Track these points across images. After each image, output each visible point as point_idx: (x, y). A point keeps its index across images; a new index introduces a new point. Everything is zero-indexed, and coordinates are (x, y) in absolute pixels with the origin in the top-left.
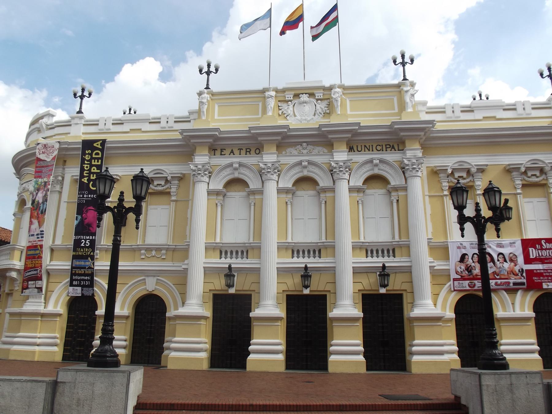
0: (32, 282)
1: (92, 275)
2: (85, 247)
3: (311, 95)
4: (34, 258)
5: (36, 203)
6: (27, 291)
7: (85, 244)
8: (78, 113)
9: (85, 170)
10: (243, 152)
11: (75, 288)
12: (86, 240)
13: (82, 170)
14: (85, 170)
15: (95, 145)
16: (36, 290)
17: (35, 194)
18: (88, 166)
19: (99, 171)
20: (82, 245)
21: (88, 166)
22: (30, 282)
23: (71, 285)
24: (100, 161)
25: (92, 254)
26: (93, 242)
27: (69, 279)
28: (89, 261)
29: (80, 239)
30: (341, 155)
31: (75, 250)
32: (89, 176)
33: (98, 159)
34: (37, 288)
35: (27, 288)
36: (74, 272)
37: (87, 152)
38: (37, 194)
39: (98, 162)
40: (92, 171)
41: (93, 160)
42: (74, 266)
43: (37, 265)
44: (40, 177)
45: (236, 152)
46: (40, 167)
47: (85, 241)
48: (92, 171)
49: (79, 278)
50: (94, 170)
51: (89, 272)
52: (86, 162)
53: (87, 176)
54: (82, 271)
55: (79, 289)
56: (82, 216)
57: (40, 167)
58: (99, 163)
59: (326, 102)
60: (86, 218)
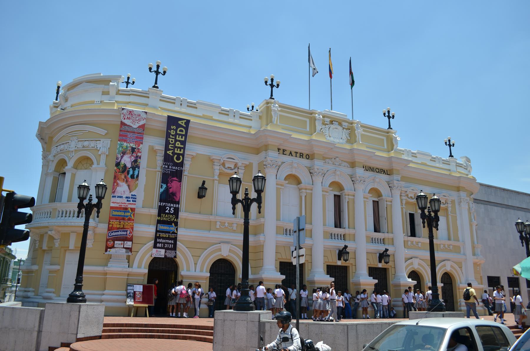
0: (120, 242)
1: (175, 239)
2: (169, 213)
3: (340, 124)
4: (124, 219)
5: (122, 166)
7: (169, 211)
8: (154, 87)
9: (170, 144)
10: (298, 155)
11: (159, 250)
12: (170, 208)
13: (167, 143)
14: (170, 144)
15: (180, 122)
16: (124, 250)
17: (119, 156)
18: (173, 140)
19: (182, 146)
20: (167, 211)
21: (173, 140)
22: (116, 242)
23: (155, 247)
24: (184, 137)
25: (175, 220)
26: (177, 211)
27: (153, 241)
28: (173, 227)
29: (165, 206)
30: (360, 172)
31: (159, 215)
32: (174, 150)
33: (182, 135)
34: (126, 248)
35: (113, 247)
36: (158, 235)
37: (172, 127)
38: (122, 157)
39: (182, 138)
40: (177, 145)
41: (177, 136)
42: (158, 229)
43: (126, 227)
44: (125, 141)
45: (294, 154)
46: (124, 131)
47: (170, 208)
48: (177, 145)
49: (164, 241)
50: (178, 144)
51: (173, 236)
52: (171, 137)
53: (172, 150)
54: (167, 235)
55: (163, 251)
56: (167, 185)
57: (124, 131)
58: (183, 139)
59: (348, 131)
60: (170, 188)
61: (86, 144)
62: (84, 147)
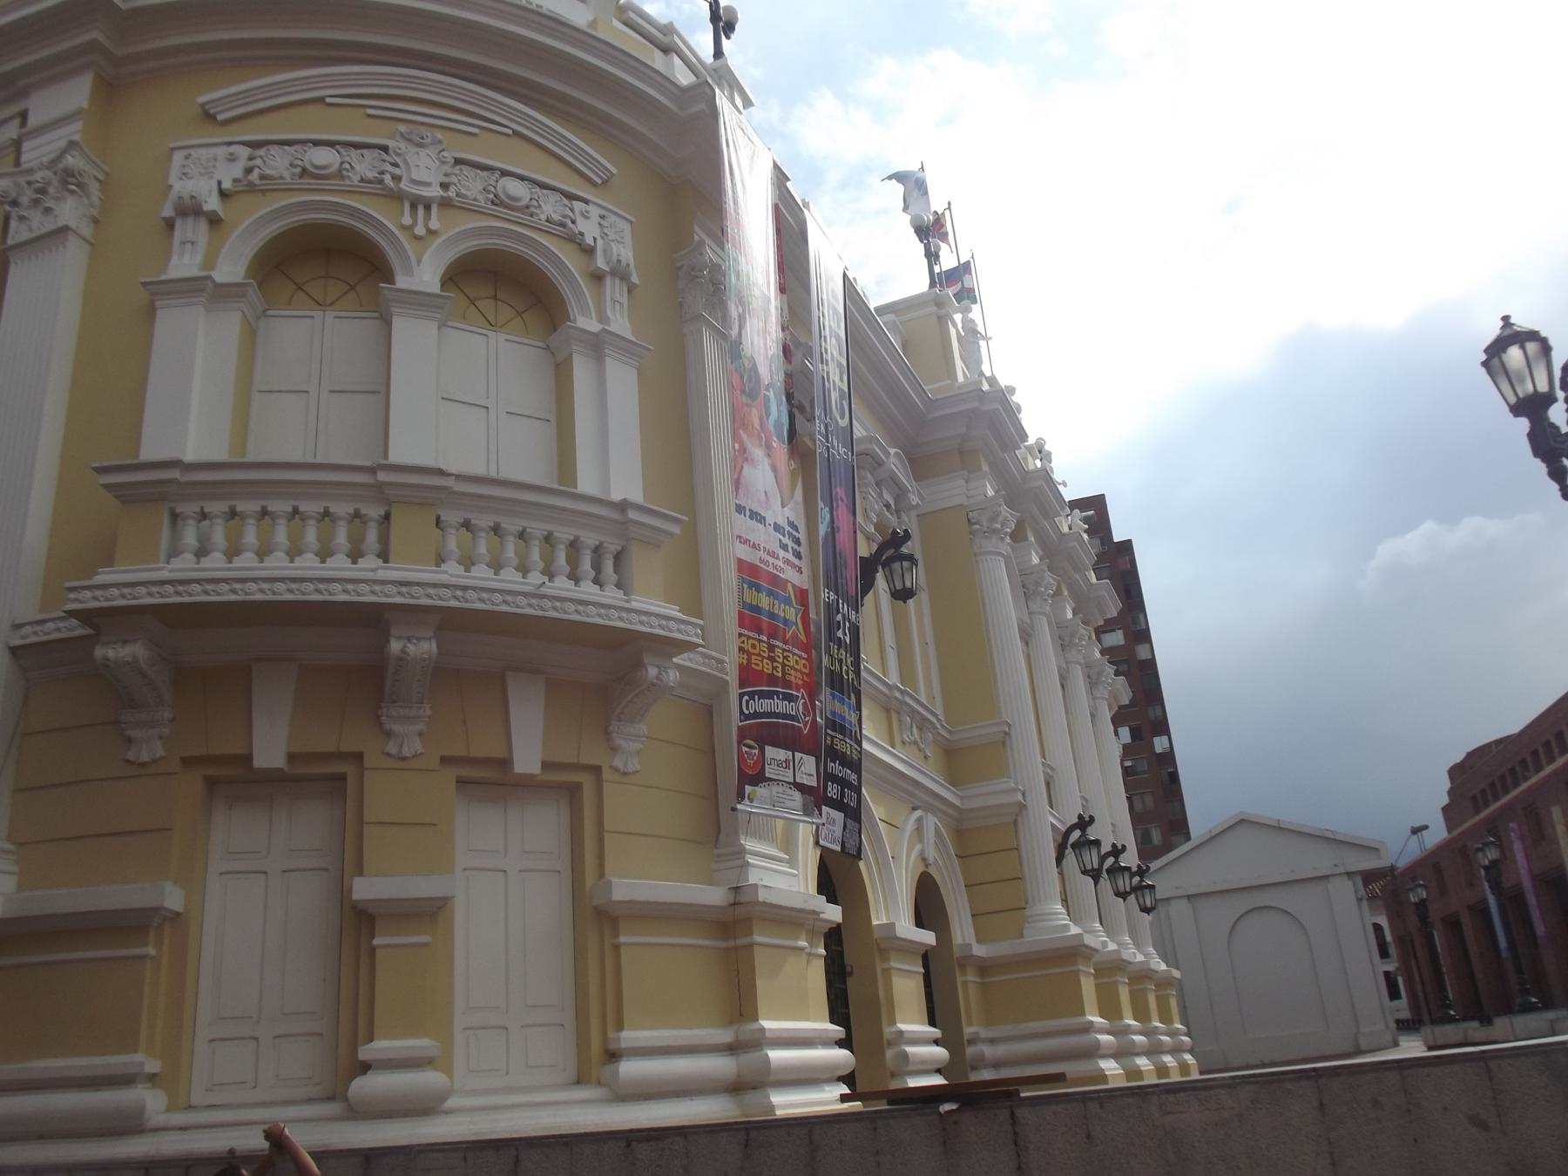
6: (761, 791)
16: (797, 795)
22: (771, 752)
34: (801, 788)
35: (759, 778)
61: (514, 188)
62: (497, 201)
